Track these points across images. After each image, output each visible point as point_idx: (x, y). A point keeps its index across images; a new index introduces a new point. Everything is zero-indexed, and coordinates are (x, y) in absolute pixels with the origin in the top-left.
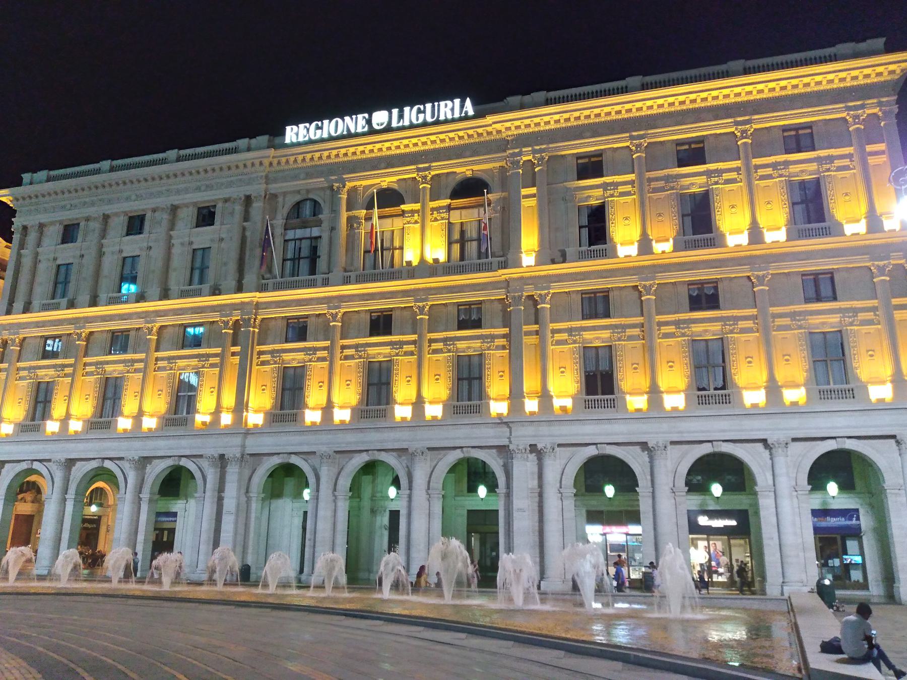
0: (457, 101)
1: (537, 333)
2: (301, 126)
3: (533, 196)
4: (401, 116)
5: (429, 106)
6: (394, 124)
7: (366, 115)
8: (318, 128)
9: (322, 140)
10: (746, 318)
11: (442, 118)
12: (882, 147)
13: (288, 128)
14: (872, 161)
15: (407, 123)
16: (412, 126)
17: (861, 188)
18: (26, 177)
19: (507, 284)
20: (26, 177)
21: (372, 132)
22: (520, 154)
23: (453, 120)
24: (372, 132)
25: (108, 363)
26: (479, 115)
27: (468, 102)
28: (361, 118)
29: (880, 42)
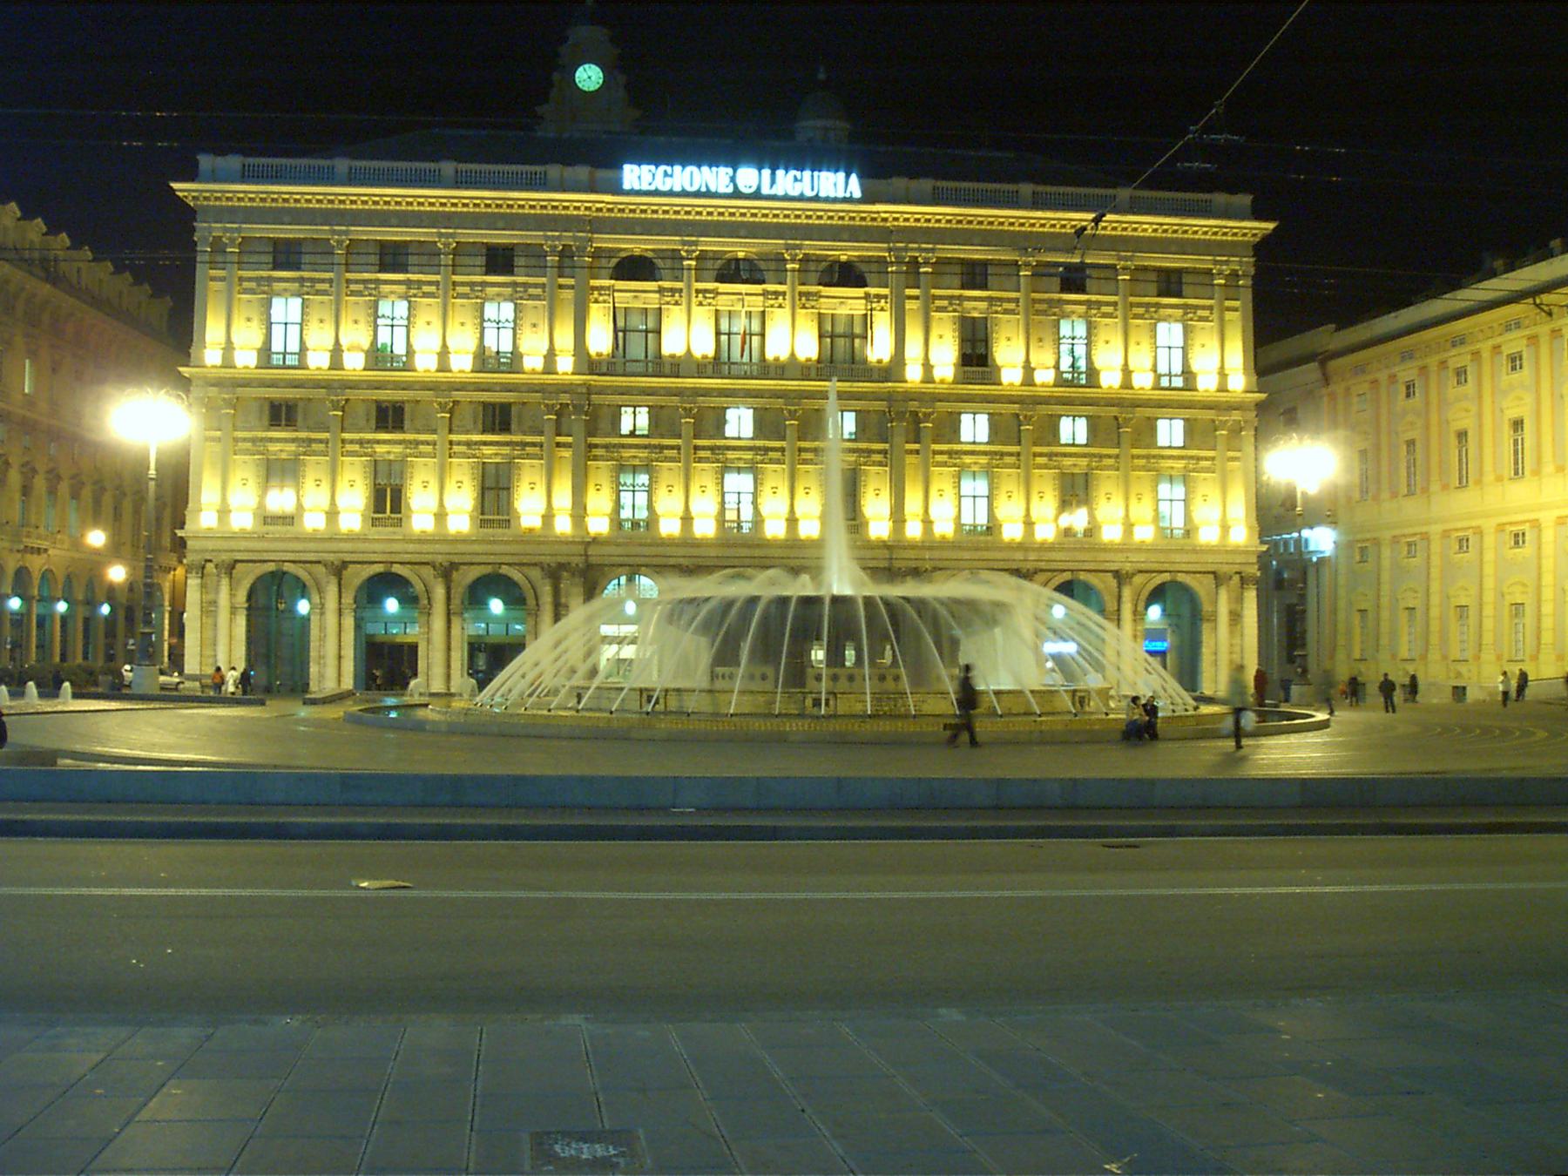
0: (841, 175)
1: (917, 452)
2: (645, 168)
3: (917, 298)
4: (773, 182)
5: (807, 174)
6: (765, 191)
7: (730, 171)
8: (666, 174)
9: (671, 194)
10: (1109, 456)
11: (822, 194)
12: (1237, 304)
13: (627, 168)
14: (1229, 315)
15: (781, 193)
16: (786, 198)
17: (1216, 343)
18: (205, 161)
19: (890, 397)
20: (205, 161)
21: (737, 194)
22: (906, 249)
23: (835, 200)
24: (737, 194)
25: (378, 442)
26: (867, 198)
27: (854, 178)
28: (724, 172)
29: (1245, 200)
